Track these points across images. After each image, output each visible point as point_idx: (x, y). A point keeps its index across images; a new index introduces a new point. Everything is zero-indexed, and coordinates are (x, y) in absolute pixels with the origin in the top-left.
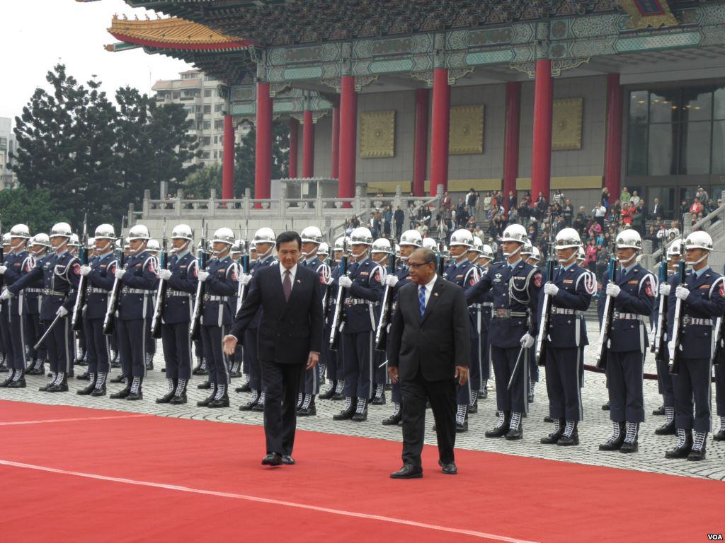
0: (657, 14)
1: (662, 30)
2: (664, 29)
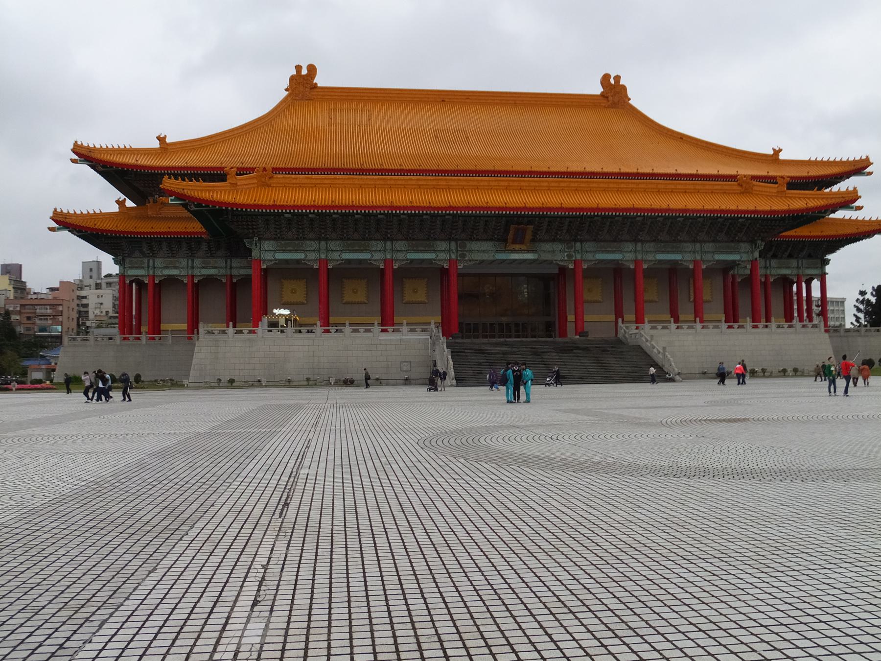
1: (521, 251)
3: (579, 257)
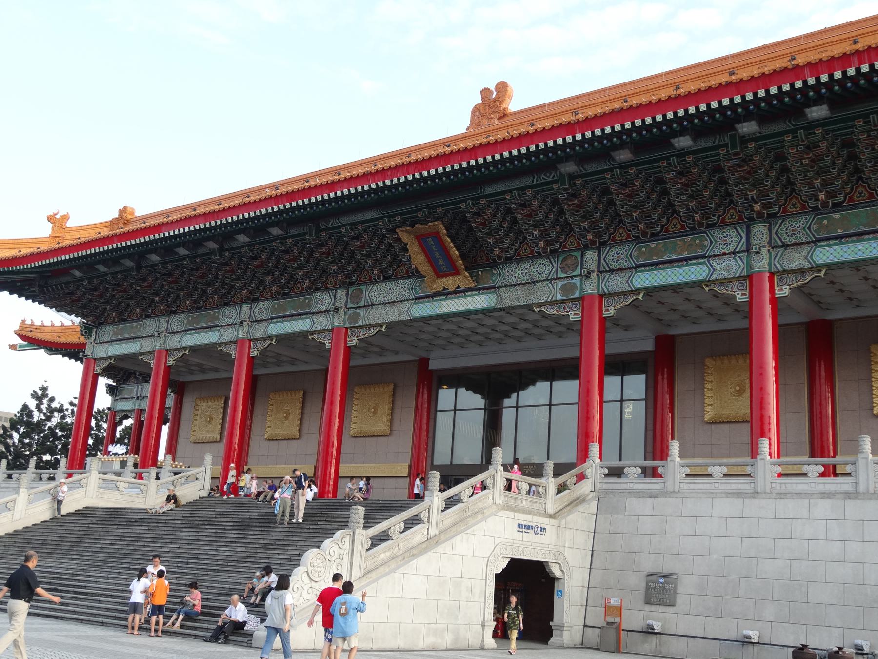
0: (452, 275)
1: (457, 292)
2: (460, 292)
3: (590, 288)
